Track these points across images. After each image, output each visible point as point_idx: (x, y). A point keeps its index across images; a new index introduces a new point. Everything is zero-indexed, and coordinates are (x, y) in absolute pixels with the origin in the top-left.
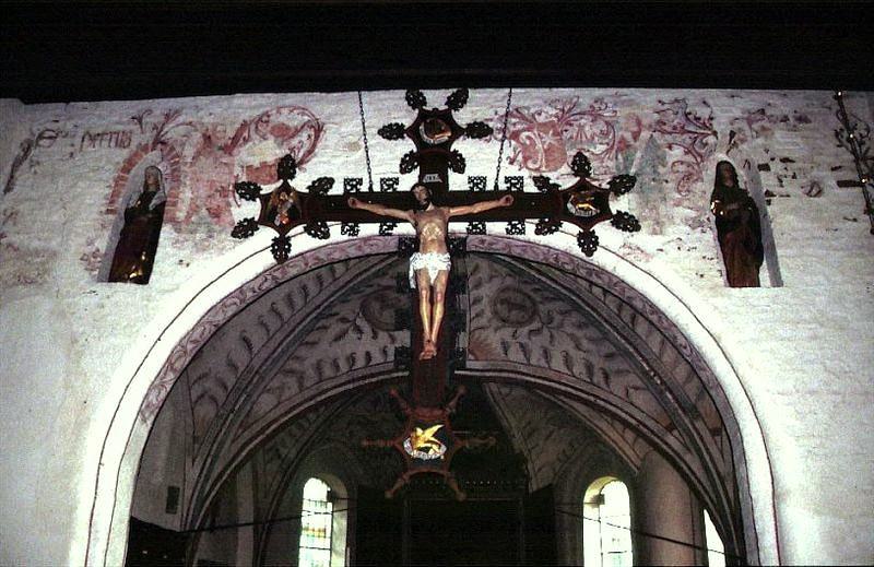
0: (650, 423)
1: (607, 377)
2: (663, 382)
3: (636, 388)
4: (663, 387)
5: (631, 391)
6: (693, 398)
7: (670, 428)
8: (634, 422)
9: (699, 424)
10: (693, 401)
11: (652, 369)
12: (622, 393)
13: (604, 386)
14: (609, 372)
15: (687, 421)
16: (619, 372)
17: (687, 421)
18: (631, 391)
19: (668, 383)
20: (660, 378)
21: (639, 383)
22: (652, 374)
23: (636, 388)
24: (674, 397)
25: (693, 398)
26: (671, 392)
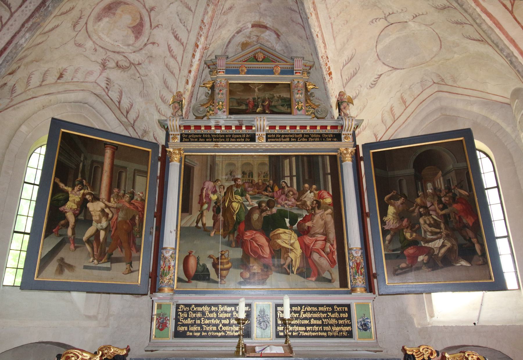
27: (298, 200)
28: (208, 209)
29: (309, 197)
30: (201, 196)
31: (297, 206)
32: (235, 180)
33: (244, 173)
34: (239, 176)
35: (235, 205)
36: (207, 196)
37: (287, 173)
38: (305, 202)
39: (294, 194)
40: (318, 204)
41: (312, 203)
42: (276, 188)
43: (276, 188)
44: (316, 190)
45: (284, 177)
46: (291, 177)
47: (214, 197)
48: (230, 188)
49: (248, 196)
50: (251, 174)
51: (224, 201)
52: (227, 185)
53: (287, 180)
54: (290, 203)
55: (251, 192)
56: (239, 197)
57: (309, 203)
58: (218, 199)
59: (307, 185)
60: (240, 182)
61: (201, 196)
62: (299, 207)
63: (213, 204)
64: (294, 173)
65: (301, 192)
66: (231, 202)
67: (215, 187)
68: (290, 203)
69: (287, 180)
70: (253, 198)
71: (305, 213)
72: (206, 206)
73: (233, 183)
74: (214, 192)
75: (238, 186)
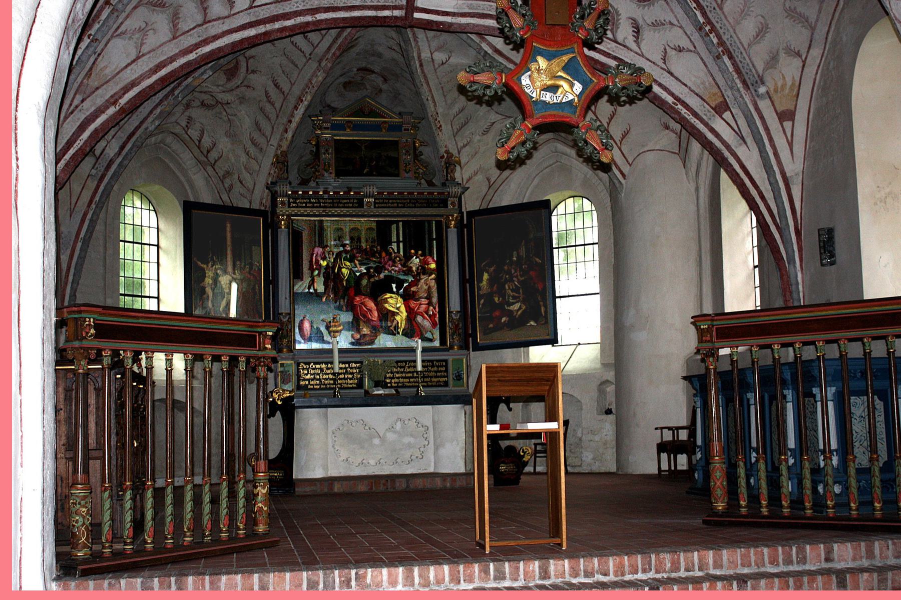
0: (693, 102)
1: (637, 31)
2: (721, 43)
3: (680, 50)
4: (720, 49)
5: (672, 53)
6: (760, 67)
7: (721, 108)
8: (670, 100)
9: (764, 105)
10: (761, 72)
11: (709, 22)
12: (657, 57)
13: (634, 46)
14: (641, 22)
15: (747, 99)
16: (657, 25)
17: (747, 99)
18: (672, 53)
19: (728, 43)
20: (719, 37)
21: (685, 43)
22: (708, 28)
23: (680, 50)
24: (735, 64)
25: (760, 67)
26: (731, 57)
27: (404, 265)
28: (319, 275)
29: (416, 261)
30: (311, 261)
31: (403, 271)
32: (344, 246)
33: (352, 239)
34: (348, 242)
35: (345, 271)
36: (317, 262)
37: (394, 239)
38: (411, 267)
39: (400, 260)
40: (424, 270)
41: (418, 268)
42: (384, 254)
43: (384, 254)
44: (421, 255)
45: (391, 243)
46: (398, 242)
47: (324, 263)
48: (339, 255)
49: (357, 262)
50: (359, 240)
51: (334, 268)
52: (336, 250)
53: (394, 246)
54: (397, 269)
55: (359, 258)
56: (348, 264)
57: (414, 269)
58: (328, 265)
59: (413, 251)
60: (348, 248)
61: (311, 261)
62: (406, 274)
63: (323, 271)
64: (401, 239)
65: (408, 257)
66: (340, 268)
67: (324, 253)
68: (397, 269)
69: (394, 246)
70: (361, 264)
71: (411, 279)
72: (316, 272)
73: (341, 249)
74: (324, 259)
75: (346, 252)
